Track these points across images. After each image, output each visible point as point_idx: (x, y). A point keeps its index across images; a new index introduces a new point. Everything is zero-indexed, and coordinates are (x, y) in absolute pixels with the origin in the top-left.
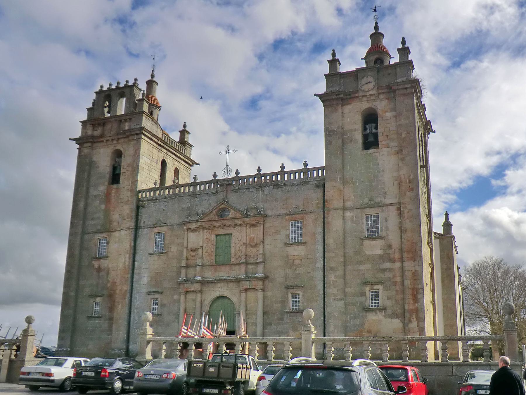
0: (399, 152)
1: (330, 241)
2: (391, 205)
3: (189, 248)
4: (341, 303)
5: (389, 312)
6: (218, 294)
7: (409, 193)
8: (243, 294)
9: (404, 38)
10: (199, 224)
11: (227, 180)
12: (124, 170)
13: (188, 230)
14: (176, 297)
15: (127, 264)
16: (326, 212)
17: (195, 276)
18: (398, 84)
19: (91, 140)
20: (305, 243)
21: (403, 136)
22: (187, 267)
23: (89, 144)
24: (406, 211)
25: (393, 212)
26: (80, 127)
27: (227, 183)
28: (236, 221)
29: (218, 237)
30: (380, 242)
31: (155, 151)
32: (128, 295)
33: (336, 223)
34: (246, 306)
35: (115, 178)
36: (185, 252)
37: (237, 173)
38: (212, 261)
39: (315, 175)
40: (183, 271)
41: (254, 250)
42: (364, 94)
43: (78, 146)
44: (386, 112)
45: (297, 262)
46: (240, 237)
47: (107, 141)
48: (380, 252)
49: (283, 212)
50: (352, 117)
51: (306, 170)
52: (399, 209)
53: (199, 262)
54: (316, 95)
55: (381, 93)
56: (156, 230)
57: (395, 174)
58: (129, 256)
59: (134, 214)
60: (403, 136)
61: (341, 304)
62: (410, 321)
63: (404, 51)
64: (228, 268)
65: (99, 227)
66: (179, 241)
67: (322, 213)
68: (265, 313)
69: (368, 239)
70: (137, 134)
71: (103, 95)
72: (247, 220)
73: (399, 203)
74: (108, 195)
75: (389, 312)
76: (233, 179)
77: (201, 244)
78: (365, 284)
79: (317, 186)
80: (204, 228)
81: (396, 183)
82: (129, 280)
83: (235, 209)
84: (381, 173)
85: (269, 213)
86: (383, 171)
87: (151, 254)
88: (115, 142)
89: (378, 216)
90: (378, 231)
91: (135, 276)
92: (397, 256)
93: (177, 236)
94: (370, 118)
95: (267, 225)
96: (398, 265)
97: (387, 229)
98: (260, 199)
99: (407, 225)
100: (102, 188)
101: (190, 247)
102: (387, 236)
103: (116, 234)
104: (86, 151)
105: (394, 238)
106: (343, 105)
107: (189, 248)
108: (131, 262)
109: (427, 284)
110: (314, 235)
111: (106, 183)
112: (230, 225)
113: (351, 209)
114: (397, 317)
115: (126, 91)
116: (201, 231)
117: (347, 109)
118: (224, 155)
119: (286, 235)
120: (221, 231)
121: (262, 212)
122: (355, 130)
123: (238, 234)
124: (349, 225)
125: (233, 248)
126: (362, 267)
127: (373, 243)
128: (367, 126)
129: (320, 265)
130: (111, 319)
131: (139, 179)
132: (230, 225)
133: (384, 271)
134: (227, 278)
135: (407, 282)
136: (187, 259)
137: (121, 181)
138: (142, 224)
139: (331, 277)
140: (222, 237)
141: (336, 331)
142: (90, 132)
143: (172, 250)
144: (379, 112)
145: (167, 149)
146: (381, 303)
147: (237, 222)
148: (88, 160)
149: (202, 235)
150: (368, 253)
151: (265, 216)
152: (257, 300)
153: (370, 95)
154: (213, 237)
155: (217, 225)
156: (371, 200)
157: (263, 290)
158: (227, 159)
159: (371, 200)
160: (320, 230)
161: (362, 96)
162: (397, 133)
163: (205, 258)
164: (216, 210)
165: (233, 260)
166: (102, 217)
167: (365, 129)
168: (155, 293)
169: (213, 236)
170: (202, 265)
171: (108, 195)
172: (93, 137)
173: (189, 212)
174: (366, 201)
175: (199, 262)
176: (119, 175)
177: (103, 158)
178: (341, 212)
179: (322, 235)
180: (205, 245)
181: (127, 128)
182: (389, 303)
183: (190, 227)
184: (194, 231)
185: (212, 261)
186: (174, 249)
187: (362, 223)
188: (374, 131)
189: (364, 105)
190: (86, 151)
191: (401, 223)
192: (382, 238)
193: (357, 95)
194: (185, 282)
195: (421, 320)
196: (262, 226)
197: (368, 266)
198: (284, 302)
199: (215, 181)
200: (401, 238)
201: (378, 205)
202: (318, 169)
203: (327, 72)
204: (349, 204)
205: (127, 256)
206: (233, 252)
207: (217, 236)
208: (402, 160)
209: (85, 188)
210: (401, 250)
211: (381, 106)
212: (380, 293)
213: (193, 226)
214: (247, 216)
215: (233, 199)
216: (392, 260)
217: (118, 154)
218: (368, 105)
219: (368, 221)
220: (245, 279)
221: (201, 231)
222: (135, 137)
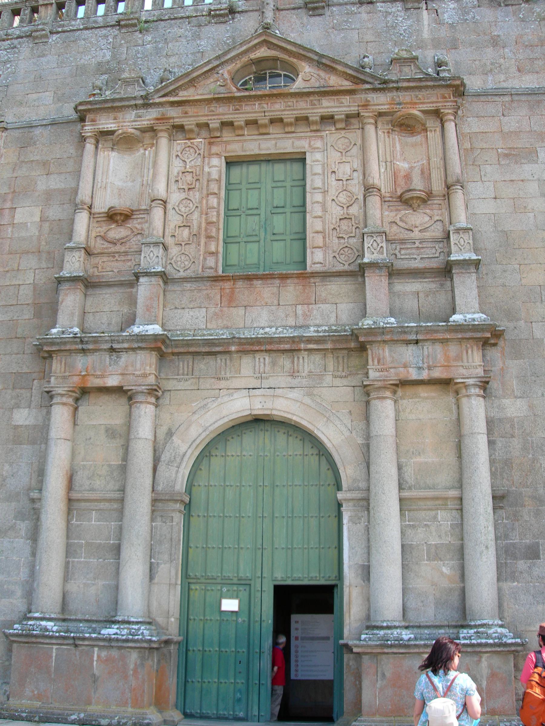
10: (152, 114)
17: (131, 321)
29: (236, 172)
36: (82, 221)
38: (211, 262)
40: (70, 301)
41: (419, 218)
46: (345, 174)
64: (291, 291)
66: (56, 182)
72: (381, 101)
93: (45, 164)
95: (473, 125)
98: (426, 35)
101: (104, 202)
123: (335, 156)
125: (313, 209)
136: (88, 252)
140: (254, 169)
143: (19, 217)
147: (328, 105)
154: (216, 166)
155: (239, 119)
163: (174, 251)
164: (230, 67)
165: (316, 259)
169: (215, 161)
180: (175, 198)
183: (111, 126)
184: (125, 142)
185: (211, 262)
206: (313, 224)
213: (128, 122)
221: (163, 142)
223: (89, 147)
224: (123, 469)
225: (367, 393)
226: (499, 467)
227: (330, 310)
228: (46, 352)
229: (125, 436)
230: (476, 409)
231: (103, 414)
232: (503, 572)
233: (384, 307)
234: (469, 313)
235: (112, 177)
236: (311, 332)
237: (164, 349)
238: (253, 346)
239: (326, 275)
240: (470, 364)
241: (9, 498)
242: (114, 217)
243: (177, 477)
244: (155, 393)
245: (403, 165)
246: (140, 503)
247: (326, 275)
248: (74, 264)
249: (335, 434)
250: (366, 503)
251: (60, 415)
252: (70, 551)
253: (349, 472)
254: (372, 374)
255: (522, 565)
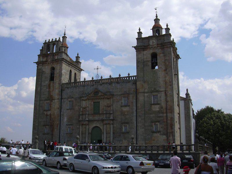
0: (165, 70)
1: (139, 105)
2: (162, 91)
3: (83, 107)
4: (143, 130)
5: (162, 133)
6: (94, 125)
7: (169, 87)
8: (105, 126)
9: (167, 24)
11: (97, 80)
12: (56, 75)
13: (82, 100)
14: (78, 127)
15: (58, 113)
16: (137, 94)
18: (166, 43)
19: (42, 63)
20: (129, 106)
21: (167, 64)
22: (82, 115)
23: (41, 65)
24: (168, 94)
25: (163, 94)
26: (37, 57)
27: (97, 82)
28: (101, 97)
30: (158, 106)
31: (67, 67)
32: (59, 126)
33: (141, 98)
34: (106, 131)
35: (52, 78)
36: (81, 108)
37: (101, 77)
39: (133, 79)
41: (109, 108)
42: (151, 46)
43: (37, 65)
44: (160, 54)
45: (126, 113)
46: (103, 103)
47: (48, 63)
48: (158, 110)
49: (120, 93)
50: (147, 54)
51: (129, 77)
52: (165, 93)
53: (87, 113)
54: (132, 47)
55: (158, 46)
56: (69, 100)
57: (164, 79)
58: (59, 109)
59: (60, 93)
60: (167, 64)
61: (143, 130)
62: (169, 136)
63: (167, 29)
64: (98, 115)
65: (46, 98)
67: (135, 94)
68: (113, 133)
69: (154, 104)
70: (61, 61)
71: (46, 44)
72: (106, 96)
73: (166, 91)
74: (49, 85)
75: (162, 133)
76: (100, 80)
77: (88, 106)
78: (152, 122)
79: (133, 83)
80: (89, 99)
81: (164, 82)
82: (59, 119)
83: (102, 93)
84: (159, 79)
85: (115, 94)
86: (159, 78)
87: (67, 109)
88: (51, 64)
89: (157, 95)
90: (157, 101)
91: (61, 118)
92: (165, 111)
94: (154, 56)
95: (114, 98)
96: (165, 115)
97: (161, 101)
99: (169, 99)
100: (47, 82)
102: (161, 103)
103: (53, 101)
104: (40, 67)
105: (163, 104)
106: (143, 51)
107: (83, 107)
108: (60, 113)
109: (176, 122)
110: (132, 102)
111: (49, 80)
112: (99, 98)
113: (147, 93)
114: (165, 135)
115: (55, 43)
116: (88, 100)
117: (145, 52)
118: (96, 70)
119: (121, 103)
120: (95, 101)
121: (112, 93)
122: (148, 61)
123: (102, 102)
124: (146, 99)
125: (100, 108)
126: (152, 116)
127: (156, 106)
128: (153, 59)
129: (135, 114)
130: (52, 135)
131: (62, 79)
132: (99, 98)
133: (160, 117)
134: (98, 119)
135: (169, 122)
137: (54, 80)
138: (63, 97)
139: (139, 119)
141: (141, 140)
142: (41, 60)
144: (158, 54)
145: (72, 66)
146: (158, 129)
147: (102, 97)
148: (41, 71)
149: (88, 102)
150: (154, 110)
151: (113, 95)
152: (110, 128)
153: (154, 47)
156: (155, 89)
157: (113, 124)
158: (97, 71)
159: (155, 89)
160: (135, 101)
161: (151, 47)
162: (165, 63)
165: (100, 112)
166: (47, 94)
167: (152, 60)
168: (69, 125)
170: (88, 114)
171: (49, 85)
172: (43, 62)
173: (82, 93)
174: (153, 89)
175: (87, 113)
176: (54, 77)
177: (47, 69)
178: (143, 94)
179: (136, 102)
181: (56, 58)
182: (161, 129)
186: (77, 108)
187: (151, 98)
188: (156, 61)
189: (151, 51)
190: (40, 67)
191: (166, 98)
192: (159, 104)
193: (149, 47)
194: (82, 121)
195: (174, 136)
196: (112, 99)
197: (154, 115)
198: (121, 129)
199: (93, 81)
200: (166, 104)
201: (158, 91)
202: (134, 76)
203: (137, 37)
204: (146, 91)
205: (58, 110)
207: (94, 102)
208: (167, 73)
209: (40, 83)
210: (166, 109)
211: (158, 51)
212: (158, 125)
213: (85, 98)
214: (106, 95)
215: (100, 88)
216: (163, 113)
217: (53, 69)
218: (154, 51)
219: (153, 97)
220: (106, 120)
221: (88, 100)
222: (60, 62)
223: (81, 101)
224: (86, 131)
225: (104, 124)
226: (113, 130)
227: (101, 117)
228: (79, 121)
229: (86, 128)
230: (112, 126)
231: (84, 126)
232: (113, 139)
233: (105, 117)
234: (112, 118)
235: (84, 104)
236: (100, 119)
237: (89, 121)
238: (95, 121)
239: (101, 114)
240: (112, 122)
241: (77, 133)
242: (84, 108)
243: (90, 131)
244: (88, 125)
245: (108, 103)
246: (87, 133)
247: (101, 114)
248: (81, 113)
249: (101, 128)
250: (103, 133)
251: (81, 126)
252: (82, 138)
253: (102, 131)
254: (104, 123)
255: (115, 138)
